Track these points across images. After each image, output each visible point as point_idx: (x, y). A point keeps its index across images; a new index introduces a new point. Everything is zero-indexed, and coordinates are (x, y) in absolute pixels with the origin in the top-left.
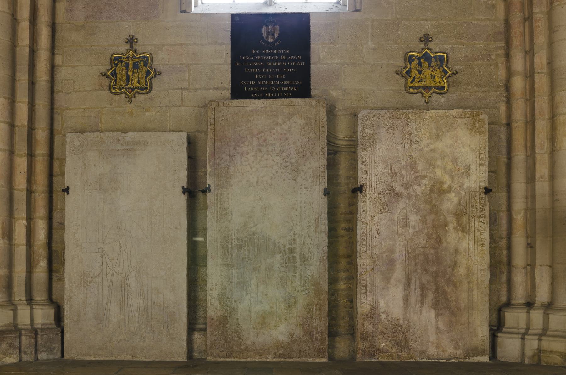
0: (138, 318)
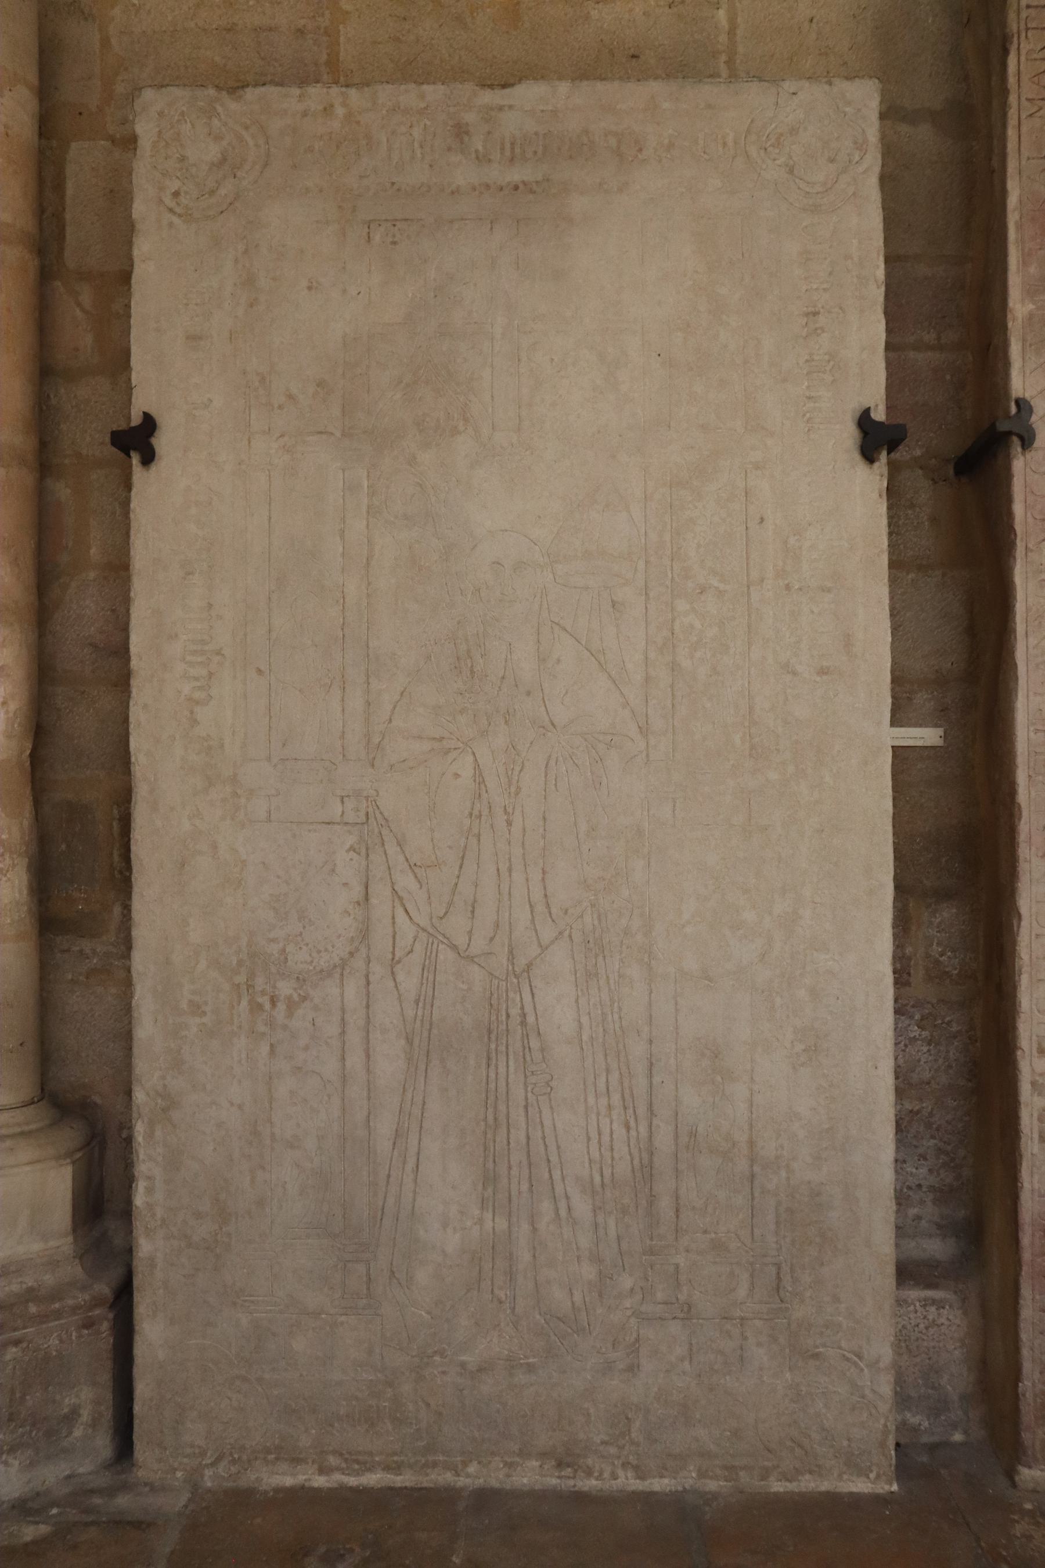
0: (596, 1225)
